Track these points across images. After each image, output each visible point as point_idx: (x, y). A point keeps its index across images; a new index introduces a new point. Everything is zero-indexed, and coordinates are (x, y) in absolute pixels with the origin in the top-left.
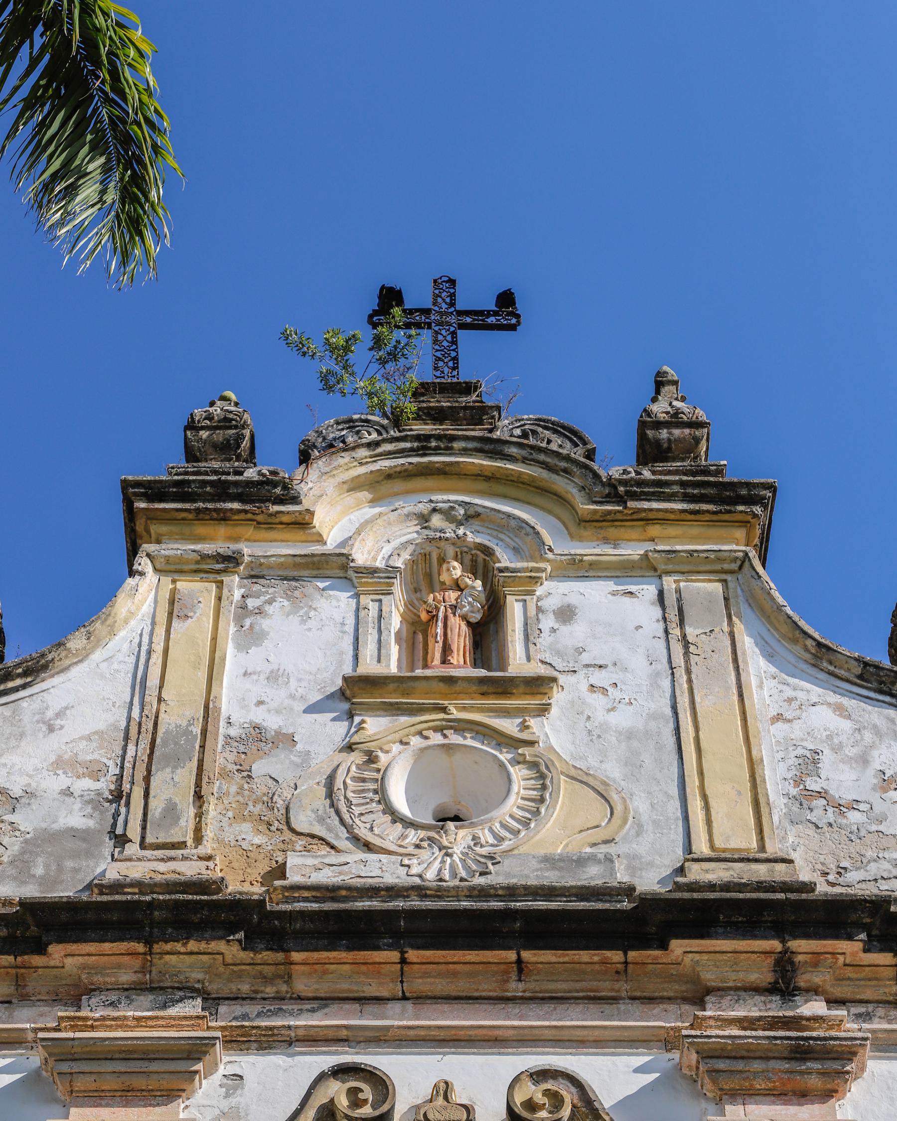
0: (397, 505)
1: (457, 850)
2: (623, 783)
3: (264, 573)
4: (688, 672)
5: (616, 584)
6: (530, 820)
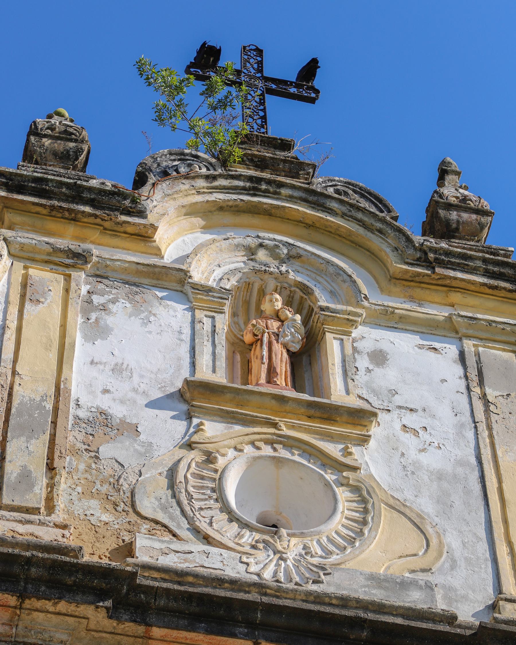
0: (228, 235)
1: (291, 555)
2: (437, 519)
3: (109, 274)
4: (490, 428)
5: (421, 338)
6: (355, 539)
